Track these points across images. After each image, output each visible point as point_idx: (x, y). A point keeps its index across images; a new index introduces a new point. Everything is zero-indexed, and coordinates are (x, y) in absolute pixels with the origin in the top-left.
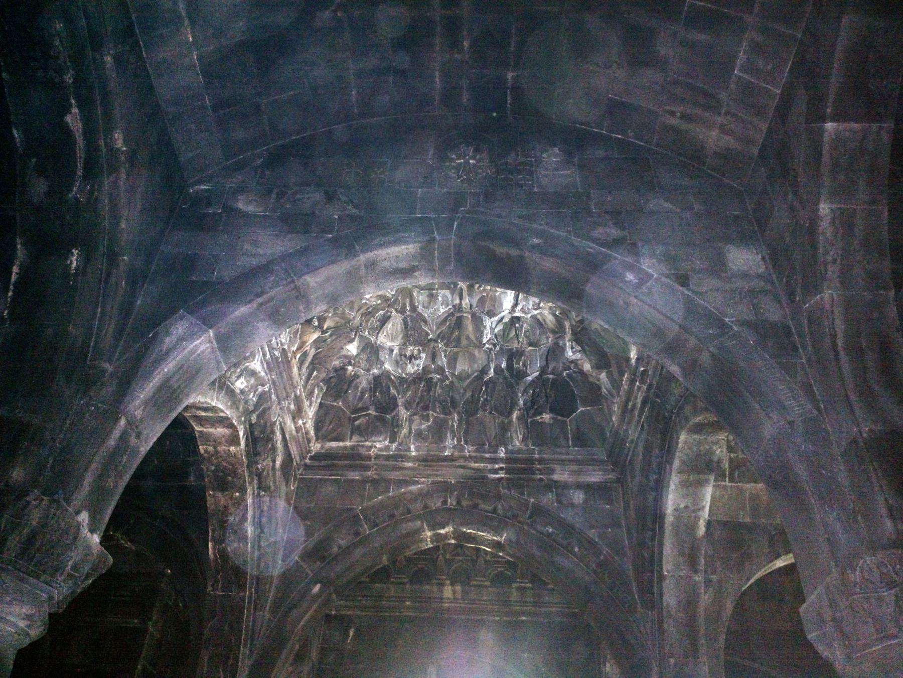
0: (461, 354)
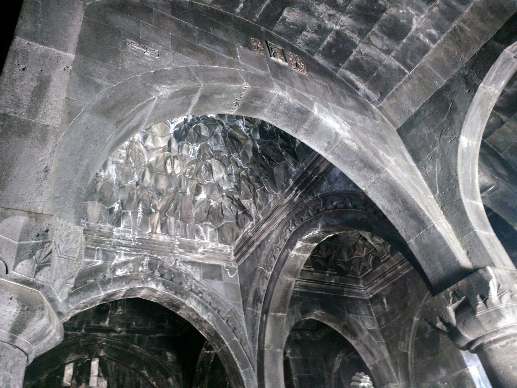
0: (245, 150)
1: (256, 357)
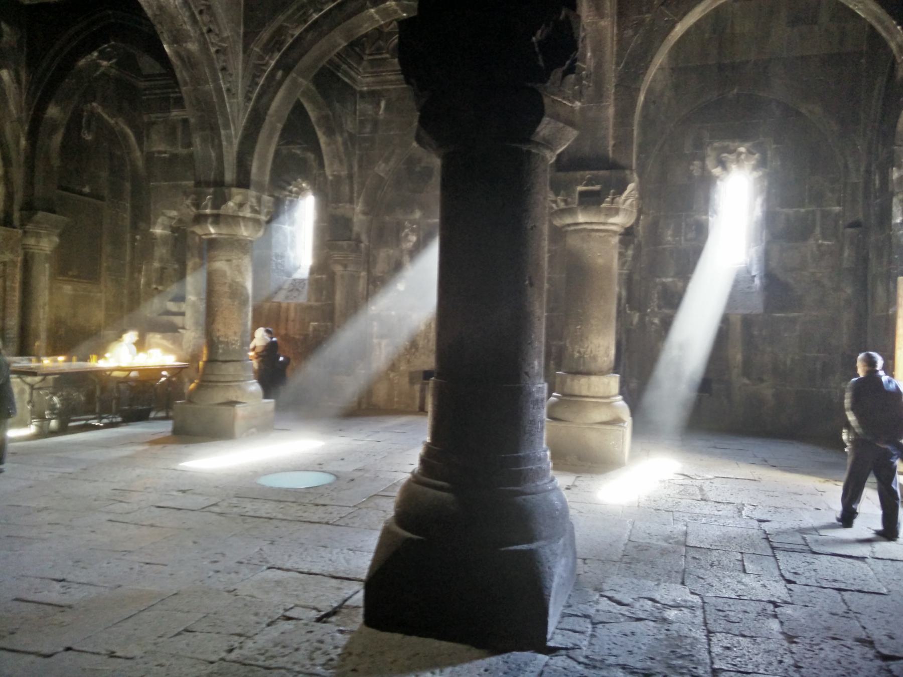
1: (245, 120)
